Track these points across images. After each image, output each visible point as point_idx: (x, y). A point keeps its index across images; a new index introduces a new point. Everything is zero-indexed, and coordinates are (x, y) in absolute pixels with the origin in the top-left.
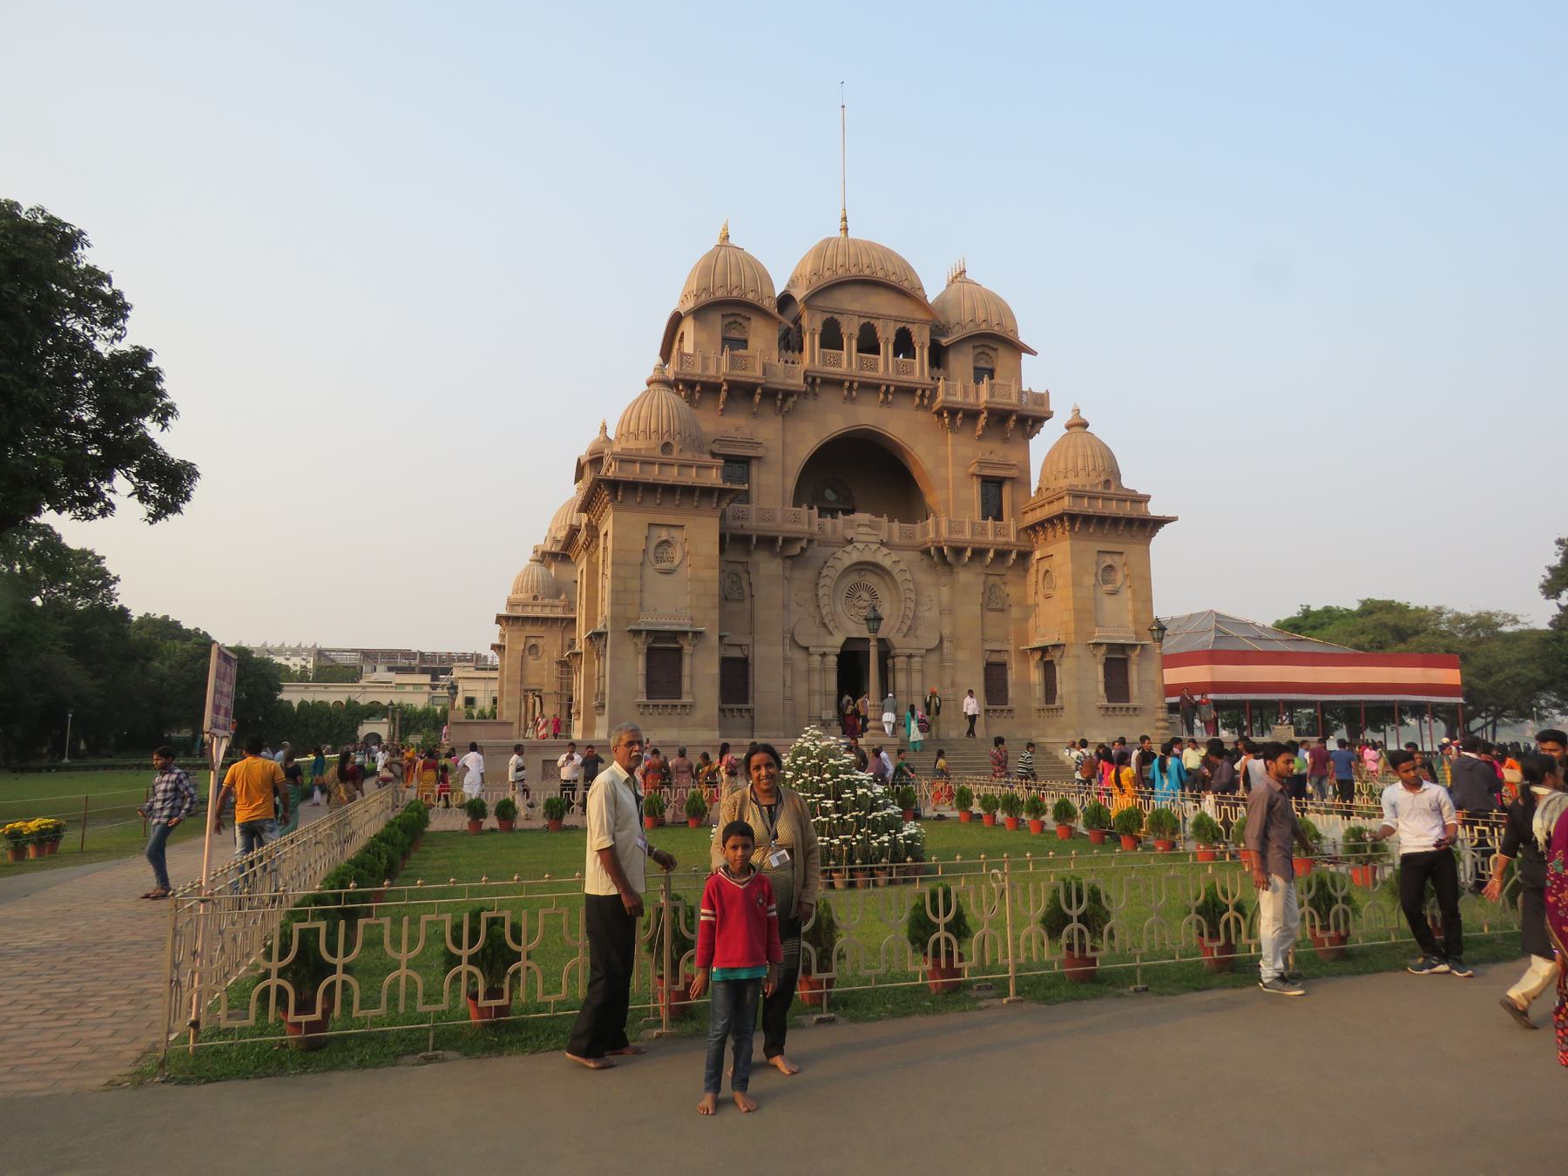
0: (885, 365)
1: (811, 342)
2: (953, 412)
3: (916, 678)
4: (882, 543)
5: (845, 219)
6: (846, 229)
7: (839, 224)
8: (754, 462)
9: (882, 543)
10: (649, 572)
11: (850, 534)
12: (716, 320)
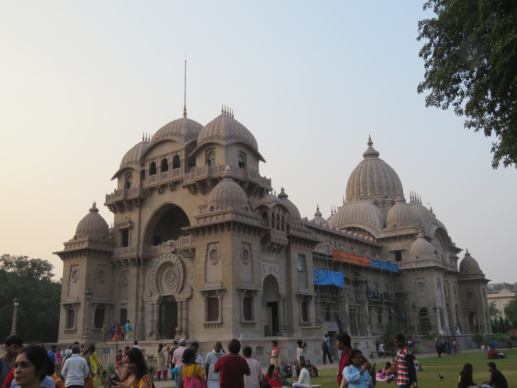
0: (170, 176)
1: (147, 174)
2: (188, 187)
4: (173, 253)
5: (185, 109)
6: (185, 114)
7: (183, 112)
8: (129, 230)
9: (173, 253)
11: (162, 250)
12: (123, 177)
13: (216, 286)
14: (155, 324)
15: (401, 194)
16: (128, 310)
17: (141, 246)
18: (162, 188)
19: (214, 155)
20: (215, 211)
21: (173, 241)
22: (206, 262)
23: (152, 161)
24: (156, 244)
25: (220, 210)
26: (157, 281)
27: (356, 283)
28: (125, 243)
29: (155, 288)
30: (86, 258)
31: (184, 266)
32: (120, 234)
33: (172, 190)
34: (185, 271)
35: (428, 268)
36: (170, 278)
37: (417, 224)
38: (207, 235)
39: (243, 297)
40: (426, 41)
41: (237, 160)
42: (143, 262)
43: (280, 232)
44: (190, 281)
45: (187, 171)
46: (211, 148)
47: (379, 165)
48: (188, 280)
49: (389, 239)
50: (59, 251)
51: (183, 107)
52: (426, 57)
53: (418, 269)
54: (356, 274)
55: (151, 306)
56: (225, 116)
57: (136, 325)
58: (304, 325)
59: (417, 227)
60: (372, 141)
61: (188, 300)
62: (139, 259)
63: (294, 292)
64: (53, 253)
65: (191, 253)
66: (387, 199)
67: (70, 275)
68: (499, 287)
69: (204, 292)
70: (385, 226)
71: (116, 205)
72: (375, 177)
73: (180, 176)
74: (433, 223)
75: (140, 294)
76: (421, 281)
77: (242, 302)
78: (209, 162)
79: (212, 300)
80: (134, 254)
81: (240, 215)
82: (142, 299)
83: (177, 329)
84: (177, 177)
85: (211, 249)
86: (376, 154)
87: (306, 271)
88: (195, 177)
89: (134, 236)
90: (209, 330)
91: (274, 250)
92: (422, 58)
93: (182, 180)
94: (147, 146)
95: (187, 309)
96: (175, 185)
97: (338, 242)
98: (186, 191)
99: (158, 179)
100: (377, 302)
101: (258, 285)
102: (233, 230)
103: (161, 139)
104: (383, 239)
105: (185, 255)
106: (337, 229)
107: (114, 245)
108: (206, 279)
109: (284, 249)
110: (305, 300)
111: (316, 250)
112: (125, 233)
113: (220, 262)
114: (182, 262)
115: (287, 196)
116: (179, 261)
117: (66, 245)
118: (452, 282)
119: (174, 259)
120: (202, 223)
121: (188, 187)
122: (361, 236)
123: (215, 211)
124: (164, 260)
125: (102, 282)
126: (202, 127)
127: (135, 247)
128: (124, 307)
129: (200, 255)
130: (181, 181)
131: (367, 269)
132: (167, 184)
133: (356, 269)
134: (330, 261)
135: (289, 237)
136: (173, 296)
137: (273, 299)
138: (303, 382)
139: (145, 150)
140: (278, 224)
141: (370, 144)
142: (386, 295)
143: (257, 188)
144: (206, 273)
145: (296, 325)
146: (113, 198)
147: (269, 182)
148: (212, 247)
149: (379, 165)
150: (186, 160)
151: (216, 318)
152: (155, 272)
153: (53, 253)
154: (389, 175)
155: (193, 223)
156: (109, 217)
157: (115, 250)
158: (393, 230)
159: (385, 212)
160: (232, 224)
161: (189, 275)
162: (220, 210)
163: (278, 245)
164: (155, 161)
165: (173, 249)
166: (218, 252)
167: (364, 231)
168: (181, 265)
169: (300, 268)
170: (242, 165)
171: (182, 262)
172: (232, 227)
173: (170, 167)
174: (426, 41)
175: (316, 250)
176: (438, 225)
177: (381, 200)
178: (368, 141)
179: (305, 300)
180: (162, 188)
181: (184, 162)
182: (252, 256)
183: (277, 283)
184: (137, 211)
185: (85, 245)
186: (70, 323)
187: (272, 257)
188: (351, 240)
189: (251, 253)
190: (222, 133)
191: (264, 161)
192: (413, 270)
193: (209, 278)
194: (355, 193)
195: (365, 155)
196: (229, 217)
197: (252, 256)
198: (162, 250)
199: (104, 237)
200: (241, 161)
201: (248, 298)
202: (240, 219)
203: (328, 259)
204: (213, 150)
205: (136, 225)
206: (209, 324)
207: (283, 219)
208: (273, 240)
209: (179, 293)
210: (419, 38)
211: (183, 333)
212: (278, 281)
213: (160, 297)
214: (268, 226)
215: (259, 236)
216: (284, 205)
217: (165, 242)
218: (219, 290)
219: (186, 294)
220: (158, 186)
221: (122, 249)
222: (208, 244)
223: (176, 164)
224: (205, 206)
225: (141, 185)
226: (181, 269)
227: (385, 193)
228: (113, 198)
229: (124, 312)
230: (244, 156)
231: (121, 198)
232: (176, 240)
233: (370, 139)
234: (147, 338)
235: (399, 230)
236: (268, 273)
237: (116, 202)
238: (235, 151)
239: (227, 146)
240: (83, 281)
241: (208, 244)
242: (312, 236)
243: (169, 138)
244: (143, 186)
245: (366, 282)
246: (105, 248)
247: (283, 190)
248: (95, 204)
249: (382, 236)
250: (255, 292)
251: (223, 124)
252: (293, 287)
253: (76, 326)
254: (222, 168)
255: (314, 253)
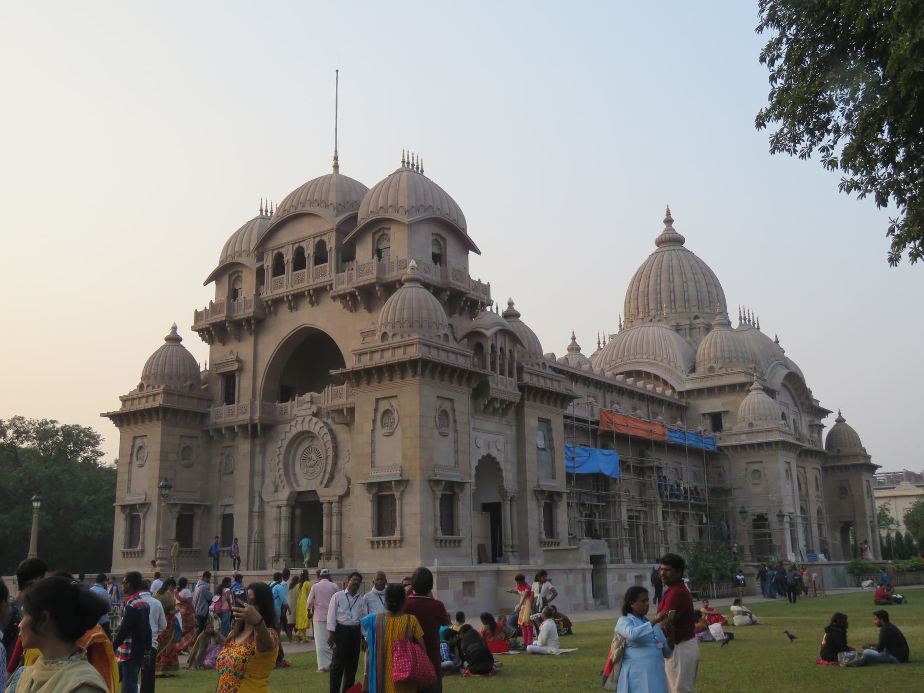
0: (310, 278)
1: (269, 273)
2: (342, 297)
3: (335, 520)
4: (315, 415)
5: (336, 158)
6: (336, 167)
7: (332, 163)
8: (237, 374)
9: (315, 415)
10: (134, 468)
11: (295, 411)
12: (226, 279)
13: (391, 475)
14: (282, 540)
15: (724, 312)
16: (235, 517)
17: (258, 402)
18: (296, 300)
19: (388, 240)
20: (390, 341)
21: (314, 394)
22: (373, 431)
23: (276, 252)
24: (284, 399)
25: (398, 339)
26: (286, 465)
27: (641, 470)
28: (230, 398)
29: (283, 477)
30: (160, 423)
31: (334, 439)
32: (220, 382)
33: (312, 303)
34: (336, 447)
35: (769, 444)
36: (310, 459)
37: (752, 365)
38: (375, 383)
39: (439, 494)
40: (772, 33)
41: (430, 250)
42: (261, 431)
43: (506, 378)
44: (346, 466)
45: (339, 270)
46: (383, 228)
47: (685, 260)
48: (341, 464)
49: (700, 392)
50: (111, 411)
51: (333, 155)
52: (772, 63)
53: (751, 446)
54: (641, 454)
55: (275, 510)
56: (408, 170)
57: (250, 542)
58: (548, 544)
59: (751, 371)
60: (673, 216)
61: (342, 498)
62: (254, 427)
63: (531, 486)
64: (102, 415)
65: (347, 416)
66: (698, 321)
67: (132, 455)
68: (895, 479)
69: (370, 486)
70: (693, 370)
71: (213, 329)
72: (677, 280)
73: (327, 278)
74: (781, 364)
75: (257, 487)
76: (756, 466)
77: (438, 503)
78: (378, 253)
79: (384, 499)
80: (245, 417)
81: (435, 347)
82: (260, 497)
83: (322, 550)
84: (321, 281)
85: (382, 409)
86: (680, 241)
87: (552, 448)
88: (354, 280)
89: (244, 385)
90: (378, 552)
91: (495, 411)
92: (765, 65)
93: (331, 285)
94: (269, 224)
95: (340, 514)
96: (318, 294)
97: (609, 397)
98: (338, 304)
99: (287, 284)
100: (677, 503)
101: (467, 473)
102: (423, 375)
103: (293, 212)
104: (690, 393)
105: (337, 420)
106: (608, 374)
107: (210, 401)
108: (373, 463)
109: (512, 410)
110: (550, 500)
111: (570, 411)
112: (229, 379)
113: (398, 432)
114: (331, 431)
115: (518, 315)
116: (326, 430)
117: (124, 400)
118: (813, 469)
119: (316, 426)
120: (366, 362)
121: (342, 297)
122: (650, 387)
123: (390, 341)
124: (299, 428)
125: (189, 466)
126: (366, 189)
127: (246, 406)
128: (228, 511)
129: (364, 418)
130: (328, 288)
131: (661, 446)
132: (304, 292)
133: (642, 444)
134: (594, 432)
135: (521, 388)
136: (314, 492)
137: (493, 498)
138: (545, 644)
139: (264, 231)
140: (502, 365)
141: (669, 221)
142: (695, 492)
143: (465, 300)
144: (373, 452)
145: (533, 544)
146: (207, 317)
147: (486, 289)
148: (384, 405)
149: (685, 260)
150: (338, 249)
151: (392, 532)
152: (283, 450)
153: (102, 415)
154: (701, 277)
155: (351, 363)
156: (201, 352)
157: (213, 410)
158: (708, 377)
159: (694, 344)
160: (420, 365)
161: (343, 454)
162: (398, 339)
163: (502, 402)
164: (283, 251)
165: (314, 409)
166: (396, 414)
167: (657, 377)
168: (329, 437)
169: (541, 443)
170: (438, 258)
171: (331, 431)
172: (419, 369)
173: (310, 262)
174: (772, 33)
175: (570, 411)
176: (787, 368)
177: (687, 322)
178: (664, 217)
179: (550, 500)
180: (296, 300)
181: (334, 253)
182: (455, 421)
183: (501, 470)
184: (251, 340)
185: (159, 401)
186: (133, 538)
187: (491, 424)
188: (632, 394)
189: (454, 416)
190: (403, 201)
191: (478, 252)
192: (743, 447)
193: (378, 462)
194: (640, 310)
195: (659, 243)
196: (414, 353)
197: (455, 421)
198: (295, 411)
199: (192, 386)
200: (437, 252)
201: (447, 495)
202: (434, 355)
203: (590, 427)
204: (386, 232)
205: (249, 366)
206: (378, 542)
207: (512, 357)
208: (492, 394)
209: (326, 486)
210: (760, 29)
211: (333, 557)
212: (502, 466)
213: (291, 493)
214: (485, 367)
215: (469, 386)
216: (512, 331)
217: (301, 395)
218: (397, 482)
219: (338, 489)
220: (288, 297)
221: (225, 408)
222: (377, 400)
223: (321, 257)
224: (372, 333)
225: (258, 294)
226: (330, 445)
227: (695, 309)
228: (207, 317)
229: (228, 520)
230: (441, 242)
231: (221, 317)
232: (320, 392)
233: (668, 213)
234: (269, 565)
235: (718, 376)
236: (483, 452)
237: (213, 325)
238: (425, 235)
239: (410, 226)
240: (156, 465)
241: (377, 400)
242: (562, 386)
243: (308, 209)
244: (262, 296)
245: (659, 469)
246: (192, 406)
247: (511, 304)
248: (175, 328)
249: (688, 386)
250: (461, 485)
251: (404, 184)
252: (529, 477)
253: (143, 543)
254: (403, 264)
255: (566, 417)
